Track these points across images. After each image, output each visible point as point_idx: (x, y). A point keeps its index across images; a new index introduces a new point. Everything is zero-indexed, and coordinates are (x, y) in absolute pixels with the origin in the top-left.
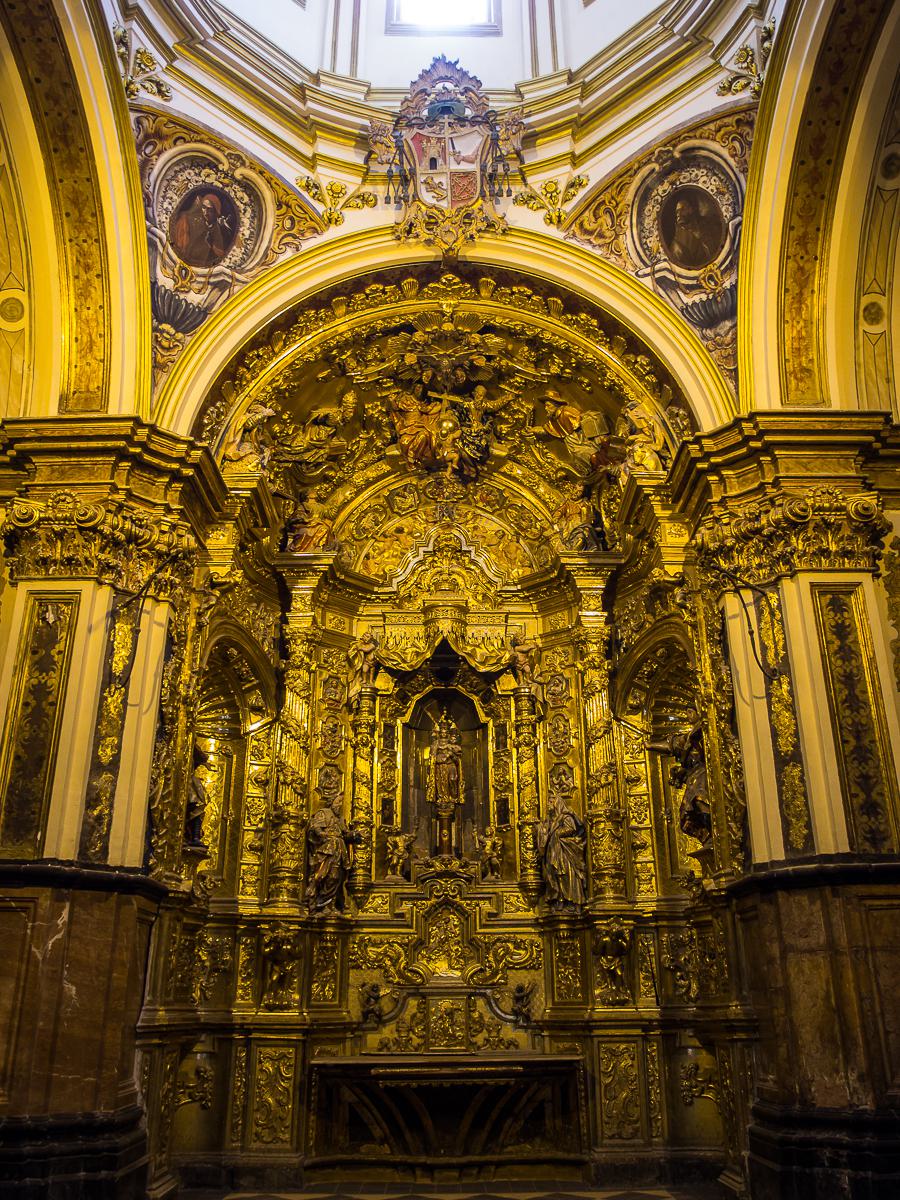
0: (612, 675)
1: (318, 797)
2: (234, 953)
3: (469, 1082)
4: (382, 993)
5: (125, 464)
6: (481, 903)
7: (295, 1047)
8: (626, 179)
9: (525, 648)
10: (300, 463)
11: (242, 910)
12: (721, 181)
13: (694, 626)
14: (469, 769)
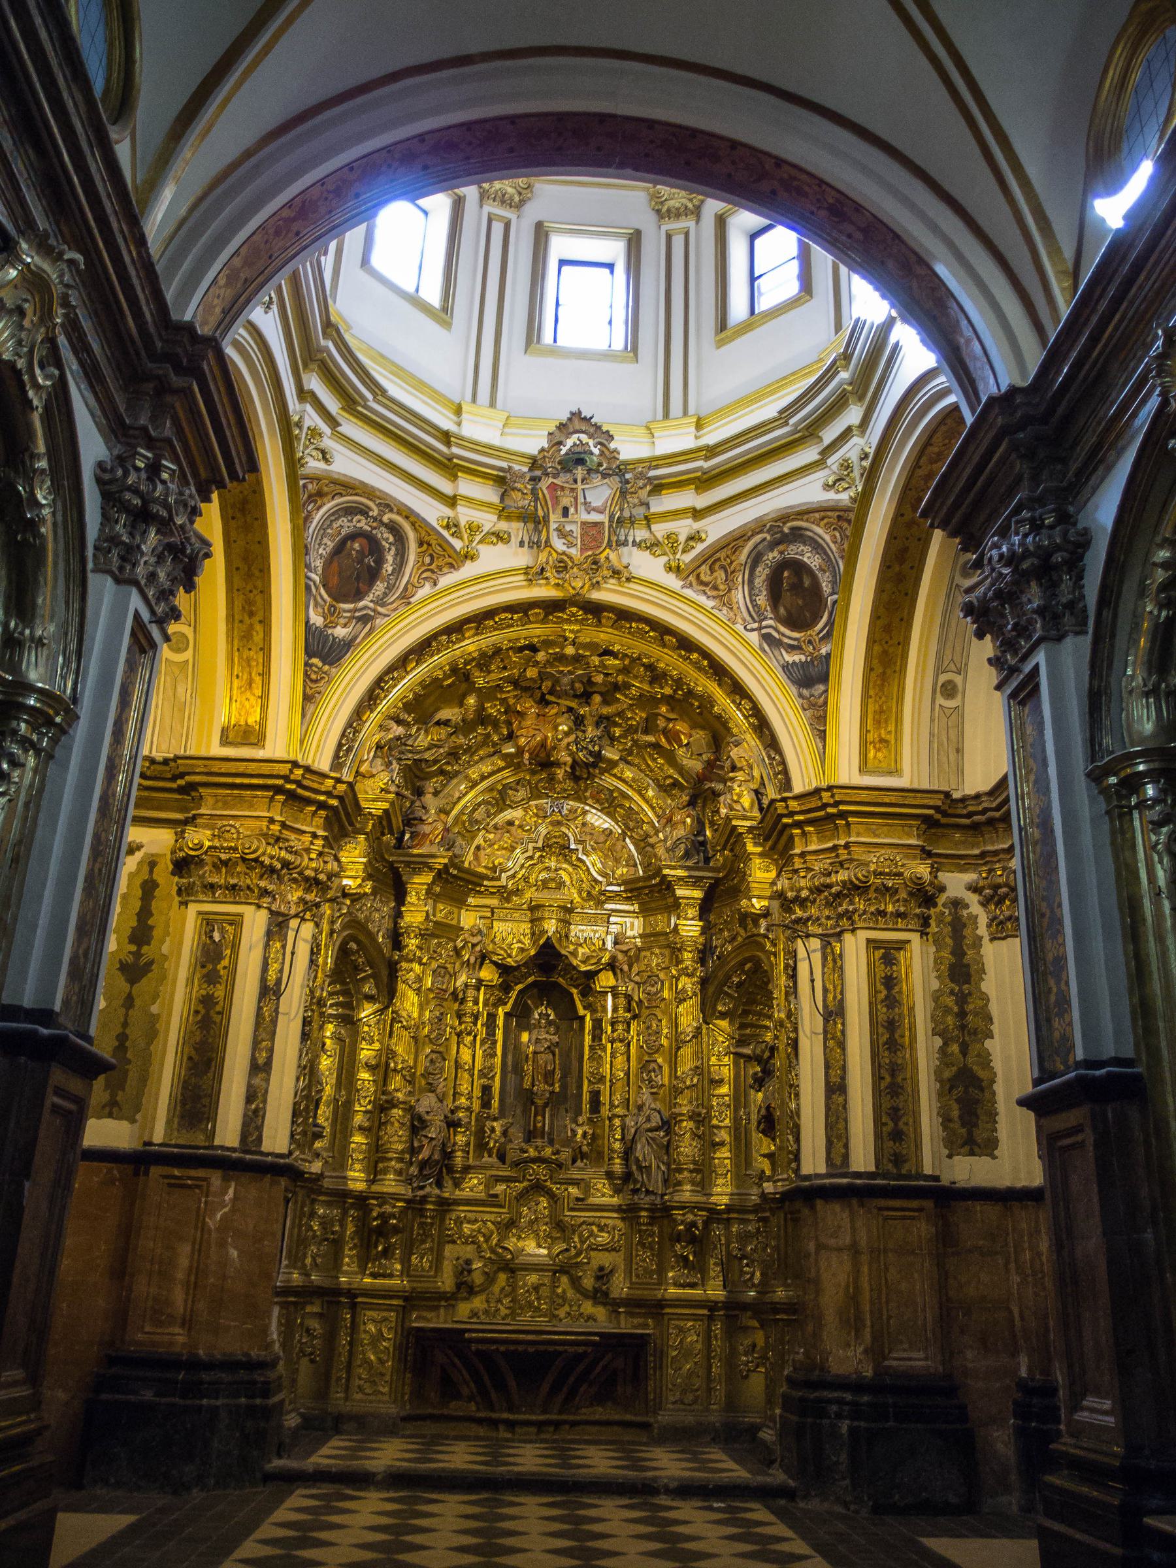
0: (704, 982)
1: (423, 1082)
2: (343, 1225)
3: (551, 1348)
4: (474, 1267)
5: (280, 797)
6: (571, 1189)
7: (397, 1311)
9: (624, 948)
10: (421, 760)
11: (352, 1185)
13: (775, 954)
14: (566, 1056)
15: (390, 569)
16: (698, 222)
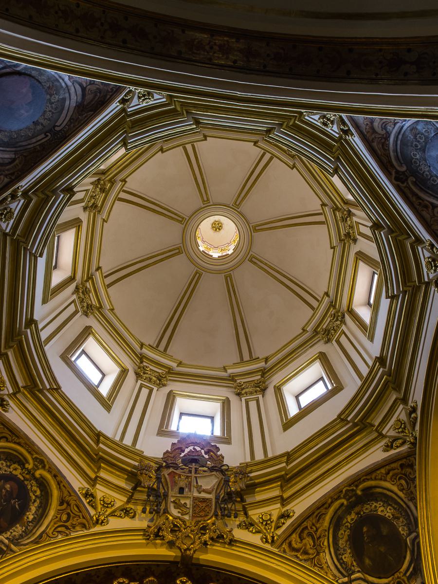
8: (323, 510)
12: (395, 509)
15: (31, 517)
16: (263, 397)
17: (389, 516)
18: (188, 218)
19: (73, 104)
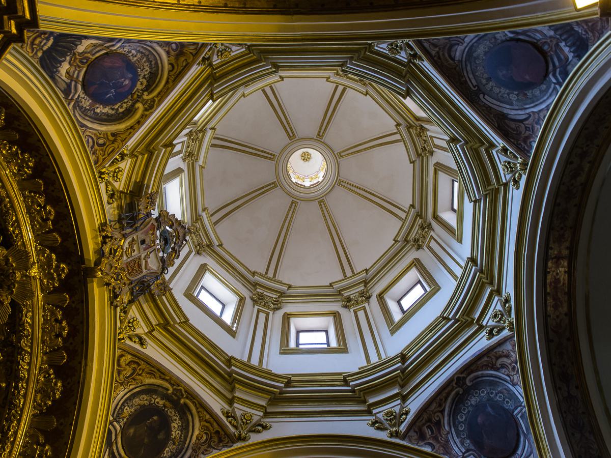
12: (180, 438)
15: (98, 111)
17: (172, 435)
18: (322, 141)
19: (505, 111)
